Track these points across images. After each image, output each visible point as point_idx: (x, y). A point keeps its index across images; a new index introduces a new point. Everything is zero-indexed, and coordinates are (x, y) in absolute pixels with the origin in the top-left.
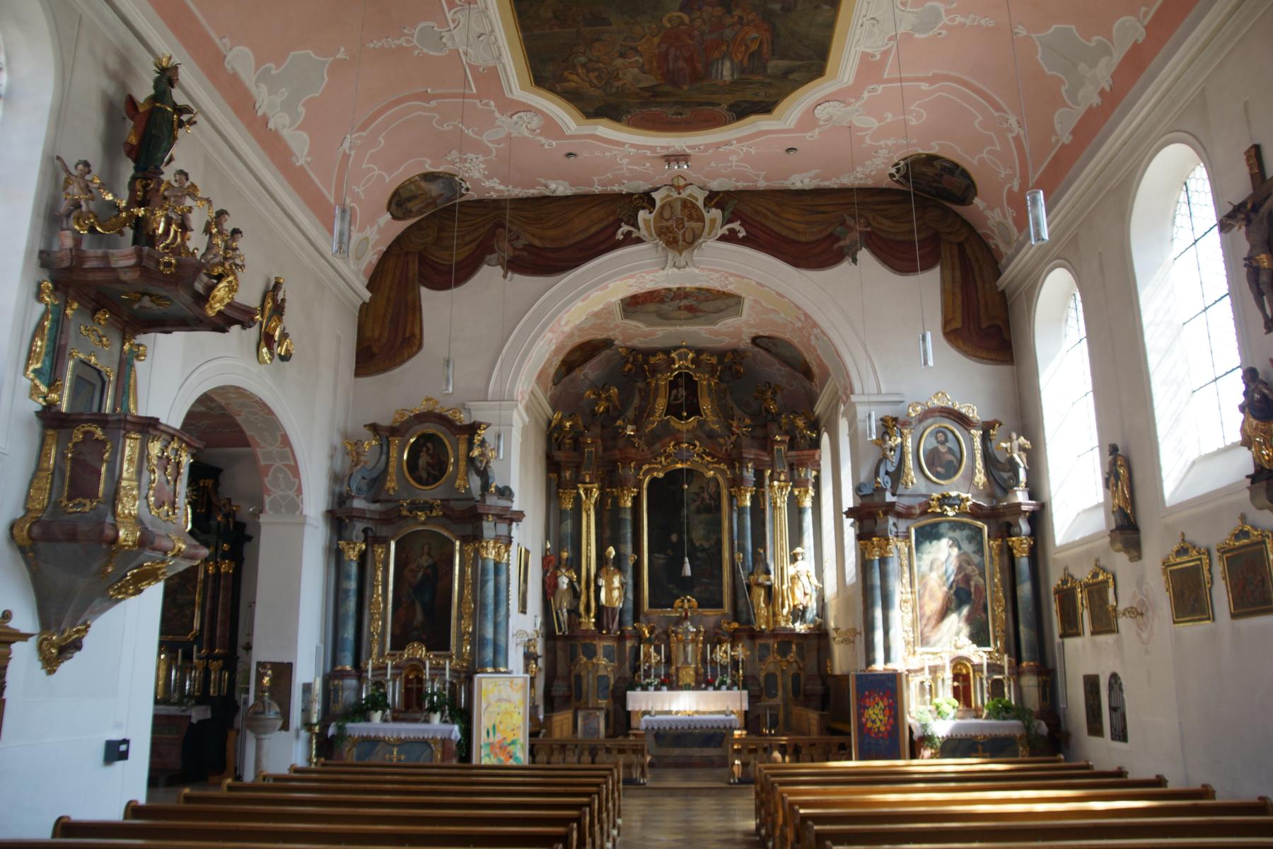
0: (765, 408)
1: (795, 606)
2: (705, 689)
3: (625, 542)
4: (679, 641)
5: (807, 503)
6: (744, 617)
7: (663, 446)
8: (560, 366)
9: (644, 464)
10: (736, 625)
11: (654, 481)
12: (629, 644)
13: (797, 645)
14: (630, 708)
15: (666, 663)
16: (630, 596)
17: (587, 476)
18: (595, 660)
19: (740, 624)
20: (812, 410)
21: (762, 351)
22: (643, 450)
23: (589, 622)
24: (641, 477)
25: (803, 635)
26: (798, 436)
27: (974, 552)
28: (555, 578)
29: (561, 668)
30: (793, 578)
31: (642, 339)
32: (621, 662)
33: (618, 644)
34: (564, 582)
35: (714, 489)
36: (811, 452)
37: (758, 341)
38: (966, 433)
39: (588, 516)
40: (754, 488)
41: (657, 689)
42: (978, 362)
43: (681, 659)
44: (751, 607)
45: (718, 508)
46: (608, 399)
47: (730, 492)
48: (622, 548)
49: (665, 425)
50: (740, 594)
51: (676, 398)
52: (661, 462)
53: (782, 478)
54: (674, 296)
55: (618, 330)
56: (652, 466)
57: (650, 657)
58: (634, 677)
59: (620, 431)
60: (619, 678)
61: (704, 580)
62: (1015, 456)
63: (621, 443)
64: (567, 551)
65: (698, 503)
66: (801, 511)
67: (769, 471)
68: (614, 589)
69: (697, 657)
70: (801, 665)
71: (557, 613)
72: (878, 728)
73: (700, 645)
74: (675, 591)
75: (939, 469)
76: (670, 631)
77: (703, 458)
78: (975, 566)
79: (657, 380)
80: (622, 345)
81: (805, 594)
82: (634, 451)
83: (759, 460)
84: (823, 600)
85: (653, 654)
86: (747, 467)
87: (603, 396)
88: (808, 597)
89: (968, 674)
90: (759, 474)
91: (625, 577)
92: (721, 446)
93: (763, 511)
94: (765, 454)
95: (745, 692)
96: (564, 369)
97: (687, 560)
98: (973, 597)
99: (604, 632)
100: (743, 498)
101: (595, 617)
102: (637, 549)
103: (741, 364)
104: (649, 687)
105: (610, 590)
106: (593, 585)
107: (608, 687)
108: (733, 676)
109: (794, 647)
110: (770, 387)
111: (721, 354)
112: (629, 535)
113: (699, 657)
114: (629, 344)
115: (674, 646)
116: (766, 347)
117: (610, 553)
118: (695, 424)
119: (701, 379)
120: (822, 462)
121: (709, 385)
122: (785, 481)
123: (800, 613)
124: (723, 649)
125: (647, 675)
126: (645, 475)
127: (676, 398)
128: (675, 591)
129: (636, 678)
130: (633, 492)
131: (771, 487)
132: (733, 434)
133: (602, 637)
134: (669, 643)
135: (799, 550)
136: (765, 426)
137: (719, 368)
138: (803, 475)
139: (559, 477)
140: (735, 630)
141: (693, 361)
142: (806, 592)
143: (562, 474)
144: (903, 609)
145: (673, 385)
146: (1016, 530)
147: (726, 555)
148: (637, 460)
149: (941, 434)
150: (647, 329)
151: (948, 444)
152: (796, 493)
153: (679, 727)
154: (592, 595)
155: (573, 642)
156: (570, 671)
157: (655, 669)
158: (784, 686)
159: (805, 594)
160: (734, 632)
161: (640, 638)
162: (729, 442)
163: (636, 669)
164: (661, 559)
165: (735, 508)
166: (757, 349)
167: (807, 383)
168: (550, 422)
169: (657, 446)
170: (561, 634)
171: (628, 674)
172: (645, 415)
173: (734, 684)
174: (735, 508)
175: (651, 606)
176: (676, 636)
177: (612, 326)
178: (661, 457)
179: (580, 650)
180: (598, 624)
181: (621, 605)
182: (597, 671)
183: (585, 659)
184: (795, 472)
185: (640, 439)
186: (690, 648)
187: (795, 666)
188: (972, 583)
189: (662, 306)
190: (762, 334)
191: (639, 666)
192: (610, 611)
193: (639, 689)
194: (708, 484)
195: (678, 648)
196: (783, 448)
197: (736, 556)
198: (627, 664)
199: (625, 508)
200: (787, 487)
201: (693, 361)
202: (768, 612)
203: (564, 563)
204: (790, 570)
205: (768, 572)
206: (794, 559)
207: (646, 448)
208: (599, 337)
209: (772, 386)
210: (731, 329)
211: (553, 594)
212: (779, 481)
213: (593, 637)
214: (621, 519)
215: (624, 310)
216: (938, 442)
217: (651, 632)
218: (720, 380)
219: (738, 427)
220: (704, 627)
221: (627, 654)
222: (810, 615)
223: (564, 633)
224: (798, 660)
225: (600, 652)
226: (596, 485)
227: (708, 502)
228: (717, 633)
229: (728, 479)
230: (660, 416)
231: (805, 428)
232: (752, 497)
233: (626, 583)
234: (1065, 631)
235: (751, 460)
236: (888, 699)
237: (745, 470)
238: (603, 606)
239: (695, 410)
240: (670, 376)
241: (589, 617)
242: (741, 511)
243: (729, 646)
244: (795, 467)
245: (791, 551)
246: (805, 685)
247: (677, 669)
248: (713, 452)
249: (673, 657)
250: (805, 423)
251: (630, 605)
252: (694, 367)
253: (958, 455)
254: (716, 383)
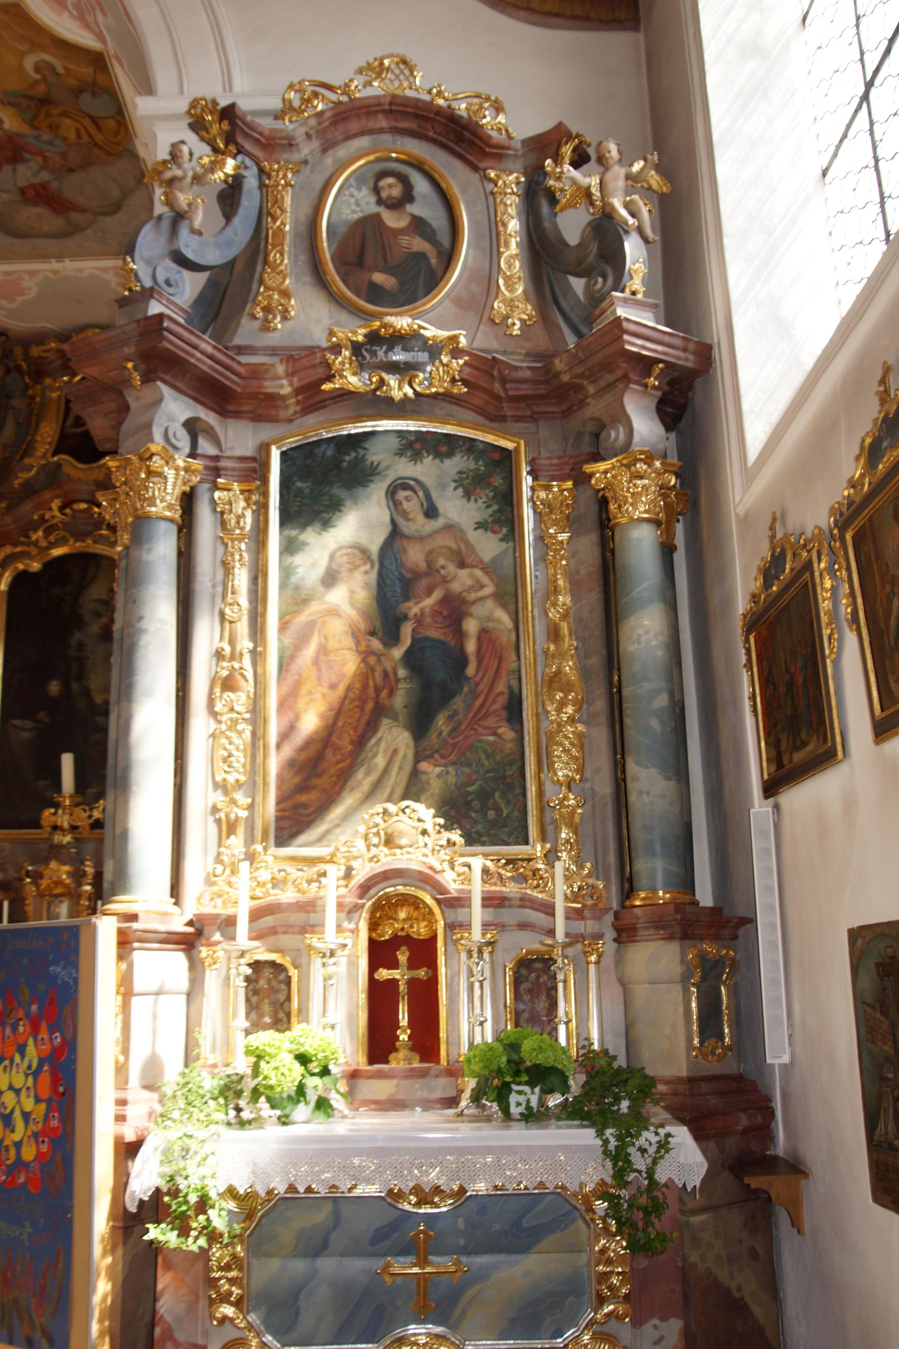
7: (38, 507)
27: (481, 525)
38: (475, 177)
42: (533, 23)
62: (617, 203)
72: (18, 1145)
75: (379, 278)
78: (485, 570)
89: (434, 938)
98: (471, 670)
144: (218, 708)
146: (617, 435)
149: (390, 180)
151: (413, 209)
169: (26, 507)
172: (18, 457)
188: (471, 626)
216: (380, 202)
230: (45, 454)
234: (780, 766)
236: (52, 1031)
253: (445, 239)
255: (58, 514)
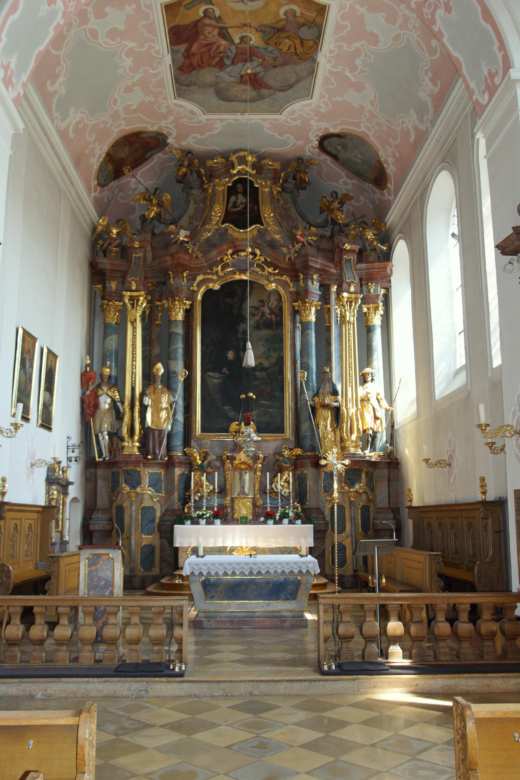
0: (332, 219)
1: (364, 431)
2: (265, 523)
3: (176, 359)
4: (235, 468)
5: (377, 320)
6: (308, 443)
7: (220, 254)
8: (105, 160)
9: (199, 274)
10: (299, 451)
11: (209, 293)
12: (178, 471)
13: (367, 473)
14: (177, 544)
15: (219, 493)
16: (180, 418)
17: (134, 284)
18: (138, 490)
19: (304, 451)
20: (383, 222)
21: (328, 159)
22: (197, 257)
23: (133, 446)
24: (195, 289)
25: (374, 462)
26: (368, 248)
28: (96, 397)
29: (102, 500)
30: (362, 400)
31: (198, 136)
32: (169, 493)
33: (166, 472)
34: (105, 402)
35: (275, 303)
36: (382, 264)
37: (326, 143)
39: (134, 328)
40: (320, 303)
41: (209, 522)
43: (238, 489)
44: (313, 431)
45: (280, 324)
46: (160, 205)
47: (294, 307)
48: (172, 364)
49: (223, 234)
50: (303, 416)
51: (235, 205)
52: (217, 272)
53: (352, 289)
54: (236, 55)
55: (171, 118)
56: (207, 277)
57: (202, 486)
58: (184, 510)
59: (172, 236)
60: (166, 510)
61: (262, 402)
63: (173, 249)
64: (110, 367)
65: (257, 318)
66: (369, 330)
67: (336, 287)
68: (162, 409)
69: (254, 486)
70: (371, 497)
71: (97, 437)
73: (259, 474)
74: (231, 414)
76: (224, 457)
77: (263, 269)
79: (214, 186)
80: (176, 146)
81: (376, 418)
82: (187, 257)
83: (326, 271)
84: (393, 427)
85: (205, 483)
86: (312, 279)
87: (155, 201)
88: (378, 422)
90: (325, 288)
91: (174, 397)
92: (284, 255)
93: (329, 329)
94: (332, 265)
95: (310, 527)
96: (110, 167)
97: (249, 345)
99: (150, 457)
100: (307, 312)
101: (139, 441)
102: (189, 365)
103: (306, 173)
104: (200, 520)
105: (157, 411)
106: (137, 403)
107: (153, 520)
108: (295, 508)
109: (363, 476)
110: (337, 197)
111: (286, 163)
112: (180, 351)
113: (257, 487)
114: (184, 144)
115: (229, 474)
116: (334, 152)
117: (158, 370)
118: (256, 232)
119: (262, 187)
120: (392, 279)
121: (271, 192)
122: (354, 293)
123: (370, 439)
124: (284, 478)
125: (198, 507)
126: (199, 286)
127: (235, 205)
128: (231, 414)
129: (186, 510)
130: (185, 304)
131: (339, 298)
132: (298, 243)
133: (146, 463)
134: (224, 471)
135: (367, 370)
136: (332, 237)
137: (283, 175)
138: (372, 290)
139: (104, 288)
140: (298, 457)
141: (254, 166)
142: (378, 414)
143: (107, 285)
145: (232, 191)
147: (288, 376)
148: (191, 269)
150: (203, 118)
152: (365, 310)
153: (238, 572)
154: (137, 415)
155: (115, 469)
156: (111, 502)
157: (207, 499)
158: (353, 519)
159: (376, 418)
160: (296, 459)
161: (190, 465)
162: (292, 251)
163: (185, 500)
164: (215, 379)
165: (298, 325)
166: (324, 157)
167: (377, 194)
168: (94, 229)
169: (214, 253)
170: (101, 460)
171: (177, 505)
173: (297, 516)
174: (298, 325)
175: (203, 430)
176: (232, 463)
177: (164, 110)
178: (217, 267)
179: (122, 478)
180: (144, 447)
181: (170, 427)
182: (142, 503)
183: (128, 488)
184: (364, 287)
185: (195, 245)
186: (247, 477)
187: (364, 497)
189: (222, 74)
190: (332, 130)
191: (190, 496)
192: (156, 433)
193: (189, 522)
194: (269, 297)
195: (233, 479)
196: (353, 257)
197: (299, 375)
198: (176, 494)
199: (176, 321)
200: (356, 299)
201: (254, 166)
202: (335, 438)
203: (106, 380)
204: (361, 392)
205: (335, 393)
206: (364, 380)
207: (200, 255)
208: (150, 129)
209: (339, 197)
210: (298, 122)
211: (93, 416)
212: (349, 292)
213: (137, 463)
214: (172, 333)
215: (177, 80)
217: (204, 458)
218: (282, 190)
219: (302, 236)
220: (262, 454)
221: (176, 483)
222: (382, 439)
223: (104, 459)
224: (368, 491)
225: (146, 481)
226: (142, 293)
227: (269, 317)
228: (278, 460)
229: (291, 292)
230: (217, 223)
231: (375, 239)
232: (317, 311)
233: (176, 403)
235: (318, 271)
237: (310, 283)
238: (149, 427)
239: (257, 219)
240: (229, 182)
241: (133, 442)
242: (305, 326)
243: (291, 474)
244: (363, 282)
245: (361, 369)
246: (374, 519)
247: (232, 500)
248: (275, 262)
249: (228, 487)
250: (374, 235)
251: (180, 428)
252: (254, 172)
254: (279, 192)
255: (230, 257)
